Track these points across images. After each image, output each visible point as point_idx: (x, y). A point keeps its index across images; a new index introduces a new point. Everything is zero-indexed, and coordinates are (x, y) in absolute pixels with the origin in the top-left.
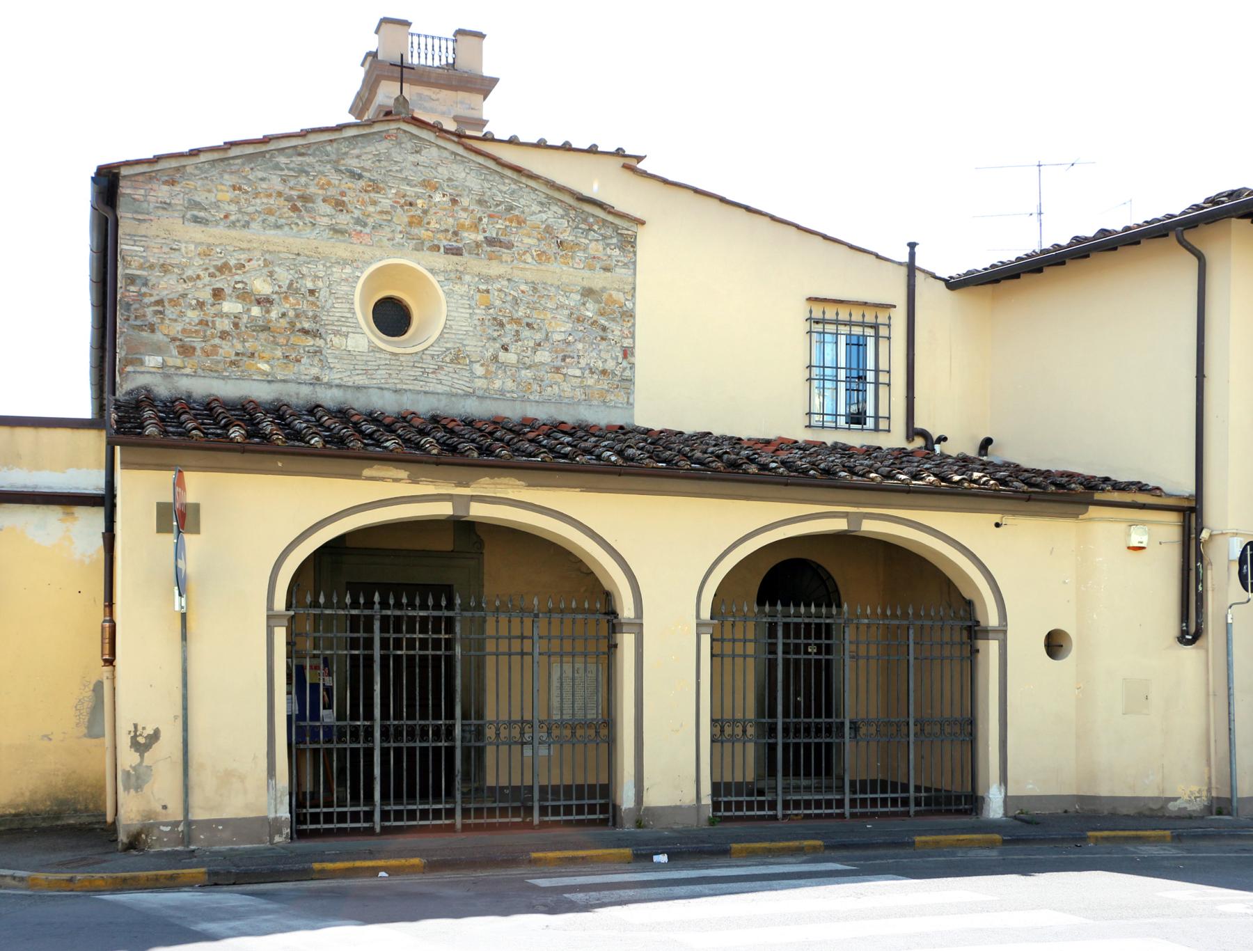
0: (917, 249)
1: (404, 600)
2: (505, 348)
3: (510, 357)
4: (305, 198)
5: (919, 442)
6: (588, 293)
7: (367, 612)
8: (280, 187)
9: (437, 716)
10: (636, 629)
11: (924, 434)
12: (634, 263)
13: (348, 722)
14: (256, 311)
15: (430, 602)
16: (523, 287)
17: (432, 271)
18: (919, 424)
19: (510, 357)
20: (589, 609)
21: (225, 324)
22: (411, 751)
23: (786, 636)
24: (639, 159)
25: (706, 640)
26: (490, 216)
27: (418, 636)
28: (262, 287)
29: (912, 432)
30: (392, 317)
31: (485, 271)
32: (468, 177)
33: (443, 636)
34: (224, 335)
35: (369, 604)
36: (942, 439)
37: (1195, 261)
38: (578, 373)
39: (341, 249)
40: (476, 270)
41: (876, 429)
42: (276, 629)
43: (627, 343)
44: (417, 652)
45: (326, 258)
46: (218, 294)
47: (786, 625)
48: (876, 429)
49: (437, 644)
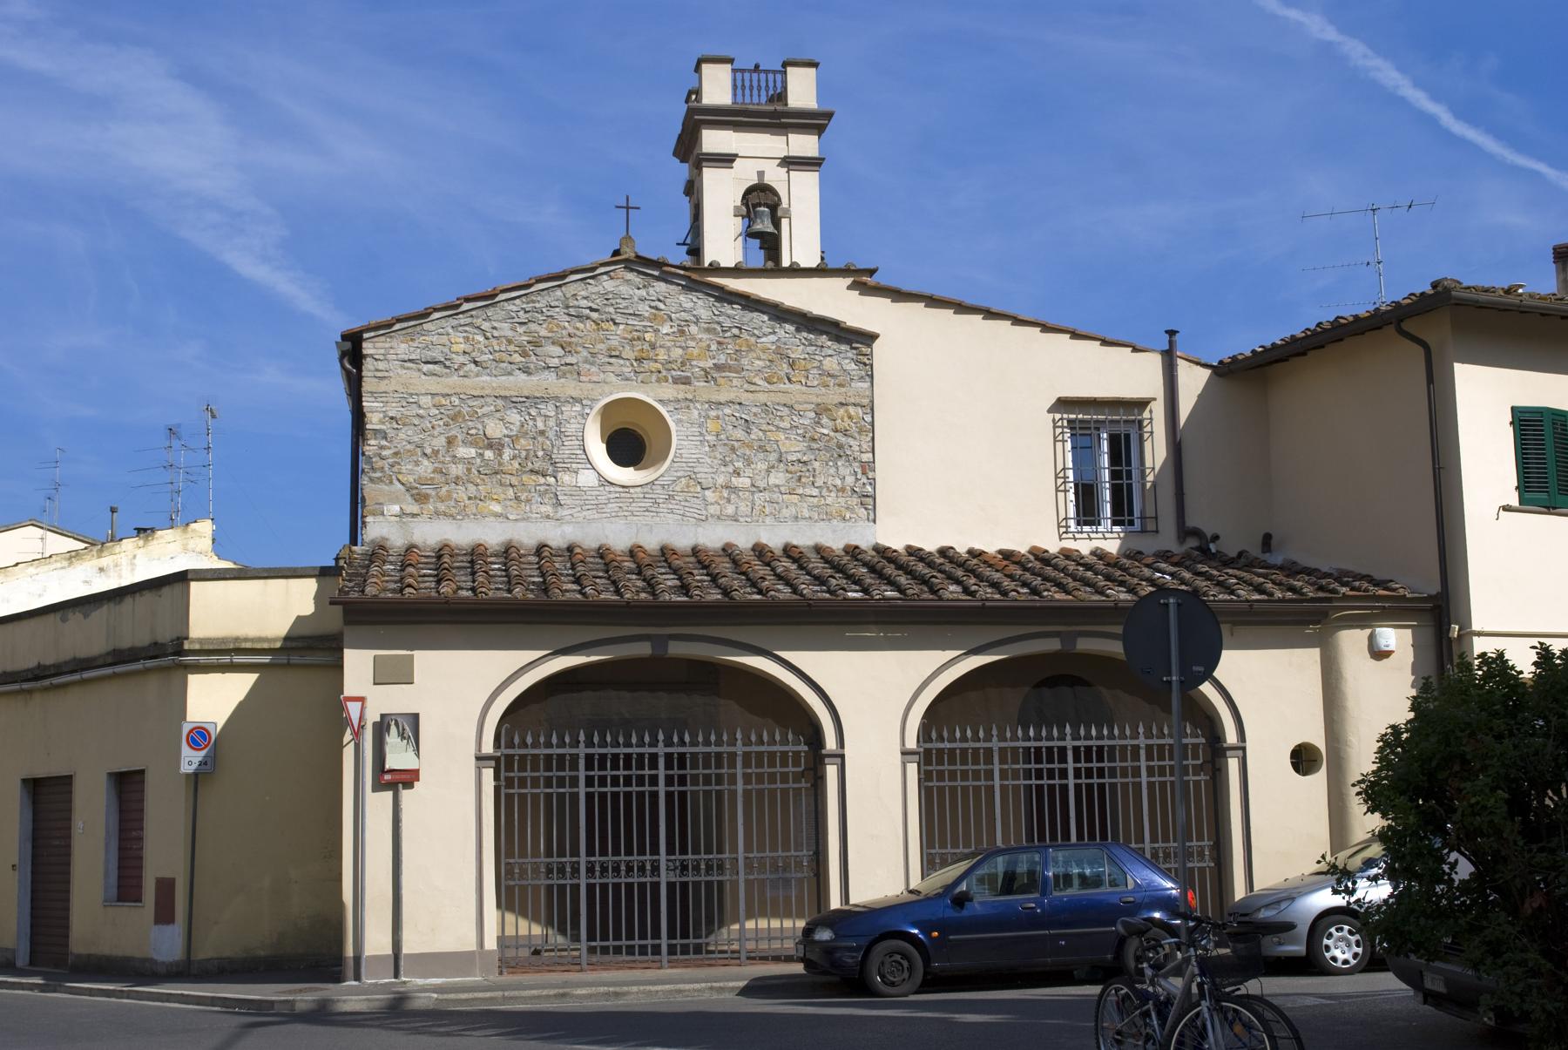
0: (1177, 337)
1: (609, 739)
2: (737, 473)
3: (743, 482)
4: (536, 344)
5: (1192, 543)
6: (821, 410)
7: (574, 751)
8: (510, 334)
9: (642, 852)
10: (839, 760)
11: (1196, 533)
12: (872, 377)
13: (555, 859)
14: (489, 454)
15: (554, 740)
16: (754, 410)
17: (660, 401)
18: (1192, 521)
19: (743, 482)
20: (801, 740)
21: (457, 470)
22: (629, 886)
23: (1077, 760)
24: (872, 272)
25: (912, 769)
26: (719, 343)
27: (622, 772)
28: (495, 429)
29: (1185, 532)
30: (629, 445)
31: (714, 398)
32: (701, 306)
33: (647, 772)
34: (457, 480)
35: (576, 744)
36: (1216, 538)
37: (1420, 350)
38: (815, 492)
39: (570, 387)
40: (705, 397)
41: (1143, 531)
42: (484, 771)
43: (867, 457)
44: (622, 789)
45: (557, 398)
46: (450, 442)
47: (1076, 749)
48: (1143, 531)
49: (641, 781)
